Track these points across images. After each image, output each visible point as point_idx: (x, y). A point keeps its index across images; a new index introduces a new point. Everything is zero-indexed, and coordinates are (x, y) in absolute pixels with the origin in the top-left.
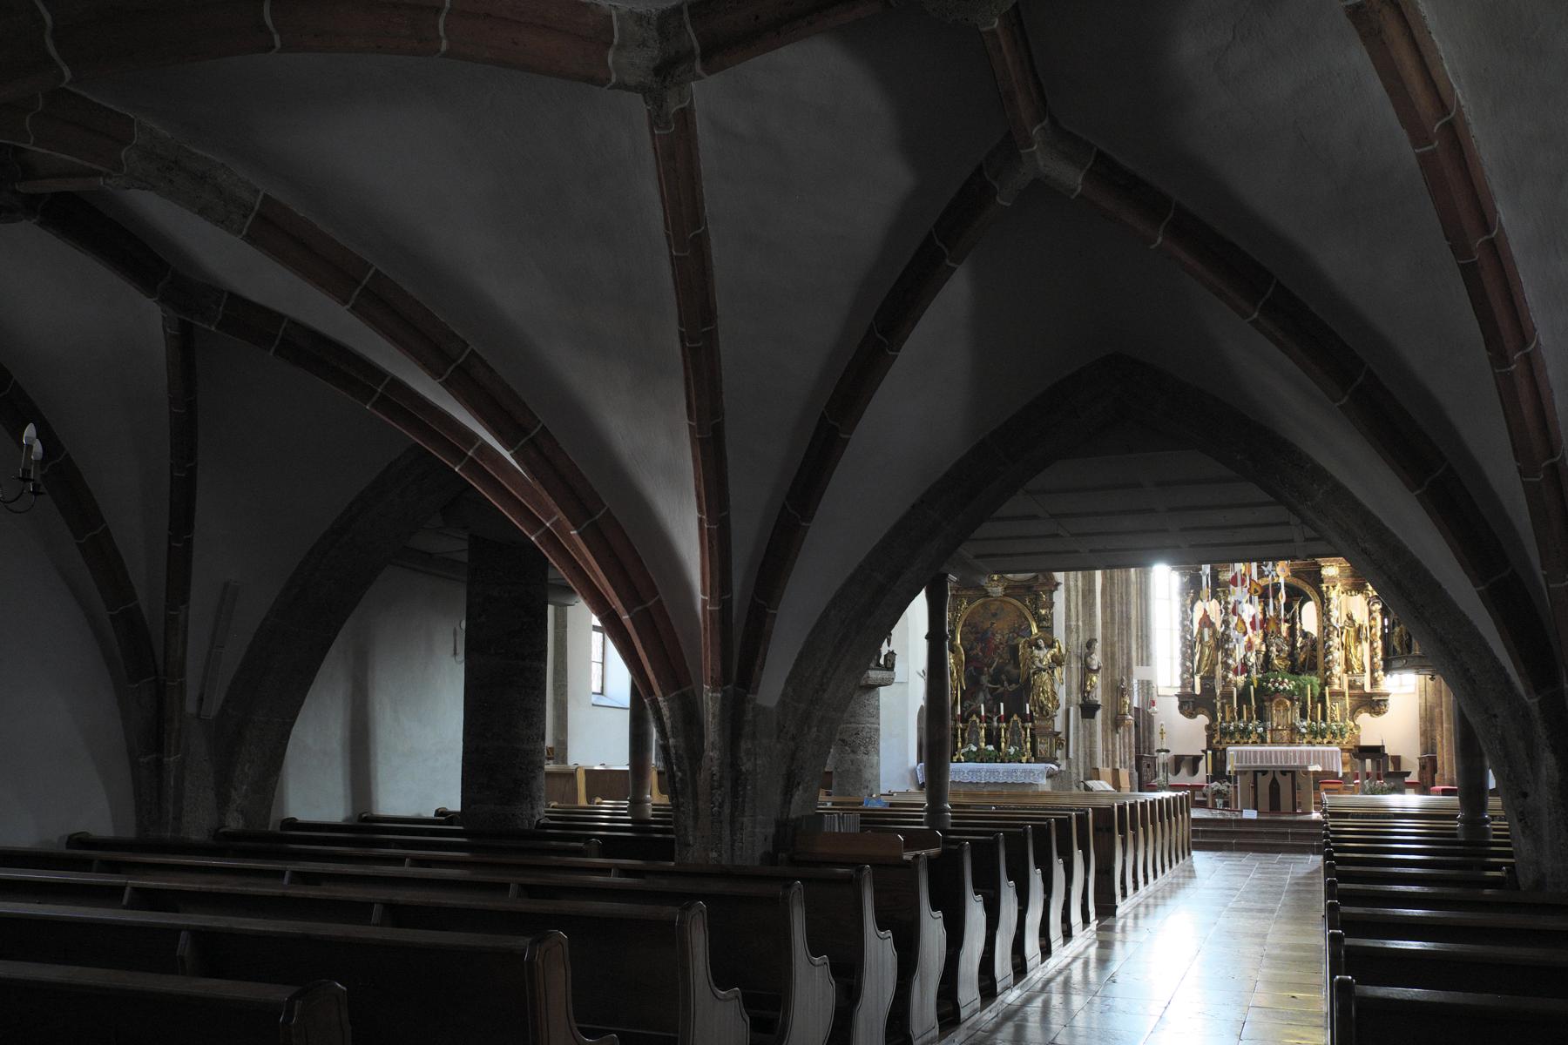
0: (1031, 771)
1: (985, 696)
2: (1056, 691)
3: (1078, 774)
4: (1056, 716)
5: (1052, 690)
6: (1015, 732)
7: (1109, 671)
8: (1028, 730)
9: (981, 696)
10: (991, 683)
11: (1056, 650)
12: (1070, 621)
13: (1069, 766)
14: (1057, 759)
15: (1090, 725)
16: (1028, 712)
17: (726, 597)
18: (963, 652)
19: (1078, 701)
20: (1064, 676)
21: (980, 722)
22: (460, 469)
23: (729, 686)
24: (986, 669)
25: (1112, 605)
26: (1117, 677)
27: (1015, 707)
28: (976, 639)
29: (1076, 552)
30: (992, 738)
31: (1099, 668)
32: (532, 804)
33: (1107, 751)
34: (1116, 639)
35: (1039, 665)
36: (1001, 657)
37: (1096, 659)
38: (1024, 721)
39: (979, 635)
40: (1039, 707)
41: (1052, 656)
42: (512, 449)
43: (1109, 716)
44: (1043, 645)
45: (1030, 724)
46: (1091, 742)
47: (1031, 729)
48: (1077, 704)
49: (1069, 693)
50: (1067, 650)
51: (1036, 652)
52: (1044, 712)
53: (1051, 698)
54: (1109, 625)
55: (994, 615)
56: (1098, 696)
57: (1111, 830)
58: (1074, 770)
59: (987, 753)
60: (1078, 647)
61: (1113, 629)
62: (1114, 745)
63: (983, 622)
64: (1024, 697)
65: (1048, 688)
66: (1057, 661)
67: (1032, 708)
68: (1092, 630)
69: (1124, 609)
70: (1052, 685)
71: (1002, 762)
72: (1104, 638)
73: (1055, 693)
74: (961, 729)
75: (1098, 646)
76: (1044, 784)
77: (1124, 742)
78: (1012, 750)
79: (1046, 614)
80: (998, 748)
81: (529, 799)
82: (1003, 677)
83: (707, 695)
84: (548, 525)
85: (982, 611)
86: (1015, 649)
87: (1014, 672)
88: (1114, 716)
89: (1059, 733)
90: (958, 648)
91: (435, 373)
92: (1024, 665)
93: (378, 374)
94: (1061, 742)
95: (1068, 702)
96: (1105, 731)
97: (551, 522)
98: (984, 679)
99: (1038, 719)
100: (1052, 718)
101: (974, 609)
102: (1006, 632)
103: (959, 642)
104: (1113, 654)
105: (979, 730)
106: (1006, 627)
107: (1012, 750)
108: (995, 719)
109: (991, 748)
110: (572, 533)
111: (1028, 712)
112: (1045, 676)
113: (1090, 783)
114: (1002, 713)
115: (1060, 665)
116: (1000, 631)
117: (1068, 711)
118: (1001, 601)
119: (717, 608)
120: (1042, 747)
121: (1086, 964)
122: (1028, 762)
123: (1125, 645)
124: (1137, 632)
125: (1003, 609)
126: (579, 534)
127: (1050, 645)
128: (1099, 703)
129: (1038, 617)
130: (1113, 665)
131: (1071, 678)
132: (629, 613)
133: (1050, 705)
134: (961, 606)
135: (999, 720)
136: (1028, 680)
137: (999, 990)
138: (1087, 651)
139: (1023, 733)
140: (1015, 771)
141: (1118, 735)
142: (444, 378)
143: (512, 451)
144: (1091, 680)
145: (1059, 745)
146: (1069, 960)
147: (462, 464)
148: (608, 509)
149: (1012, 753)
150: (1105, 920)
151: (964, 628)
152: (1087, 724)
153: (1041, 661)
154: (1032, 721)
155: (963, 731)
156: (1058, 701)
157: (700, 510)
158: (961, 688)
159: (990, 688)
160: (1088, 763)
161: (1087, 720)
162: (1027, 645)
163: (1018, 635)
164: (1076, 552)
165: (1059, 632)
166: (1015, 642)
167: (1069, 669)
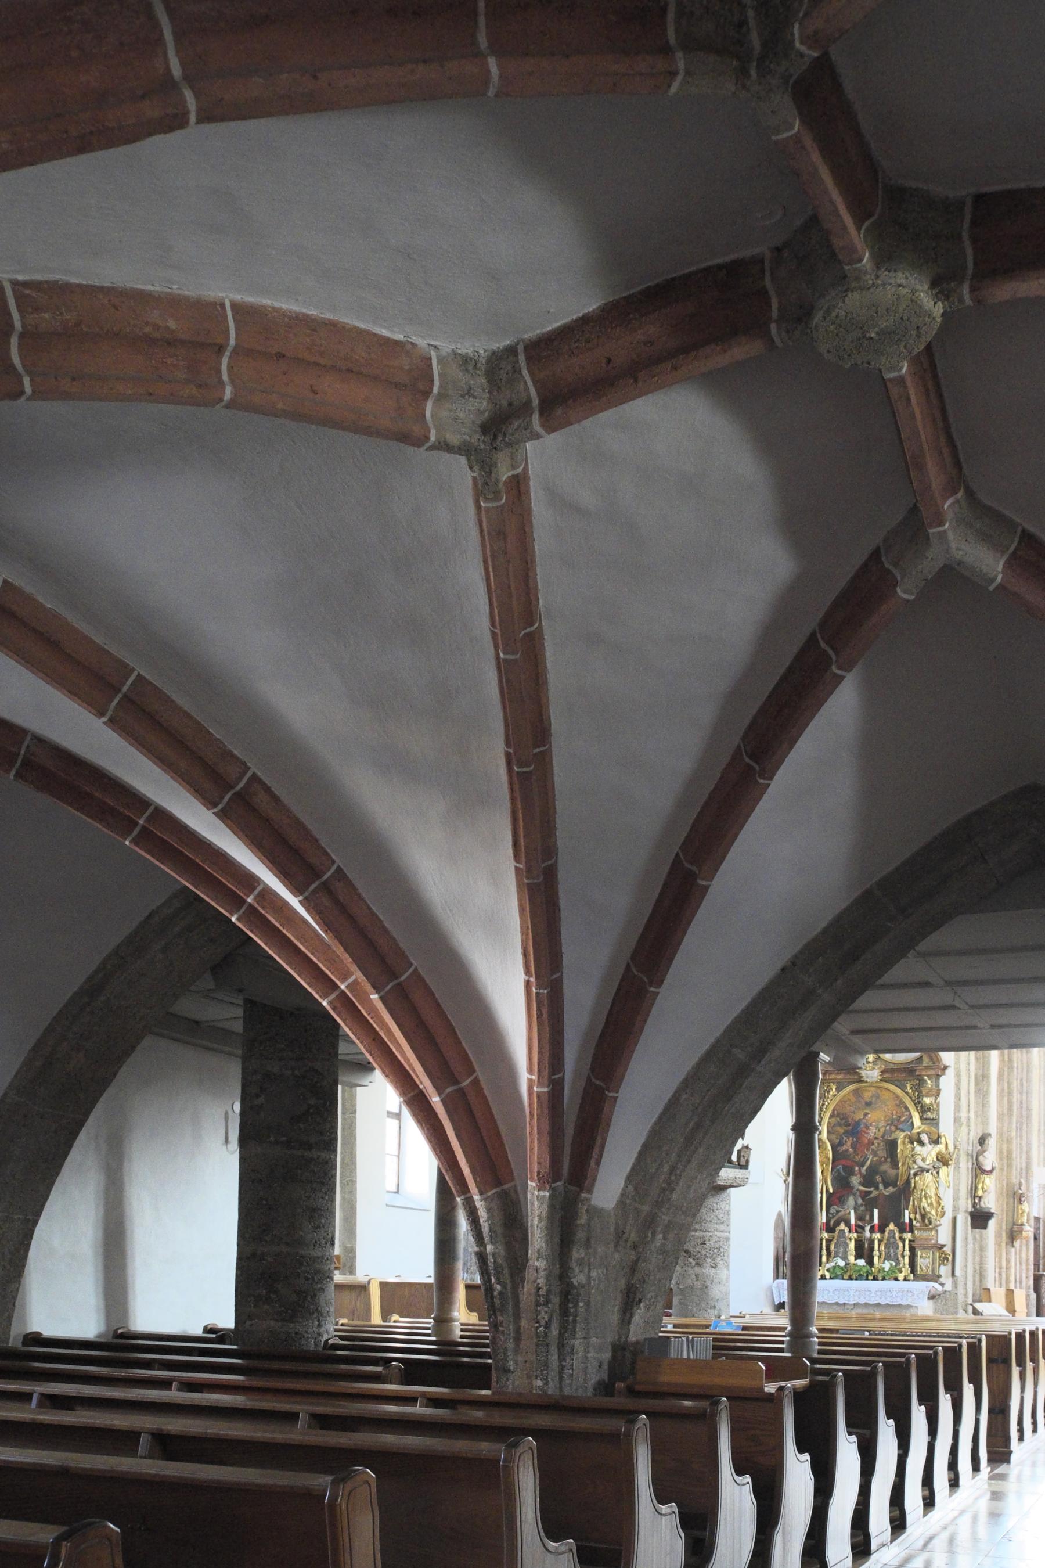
0: (909, 1291)
1: (856, 1202)
2: (941, 1196)
3: (966, 1295)
4: (940, 1225)
5: (936, 1195)
6: (891, 1244)
7: (1005, 1173)
8: (907, 1242)
9: (851, 1201)
10: (862, 1186)
11: (941, 1147)
13: (955, 1284)
14: (939, 1276)
15: (981, 1237)
16: (907, 1220)
17: (556, 1076)
19: (967, 1208)
20: (951, 1178)
21: (850, 1231)
22: (238, 919)
23: (559, 1183)
24: (857, 1168)
25: (1010, 1093)
26: (1015, 1180)
27: (892, 1212)
28: (846, 1132)
29: (975, 1027)
30: (863, 1250)
31: (993, 1169)
32: (318, 1321)
33: (1000, 1268)
34: (1014, 1134)
35: (922, 1164)
36: (875, 1153)
37: (989, 1160)
38: (902, 1231)
39: (850, 1128)
40: (921, 1213)
42: (301, 894)
43: (1004, 1227)
46: (981, 1257)
47: (910, 1241)
48: (966, 1211)
49: (956, 1199)
50: (955, 1147)
51: (918, 1149)
52: (926, 1221)
53: (935, 1204)
54: (1006, 1118)
55: (868, 1104)
56: (990, 1203)
57: (1007, 1362)
58: (961, 1291)
59: (857, 1268)
60: (968, 1144)
61: (1010, 1123)
62: (1008, 1261)
63: (854, 1112)
64: (903, 1202)
65: (931, 1192)
66: (943, 1160)
67: (912, 1216)
68: (985, 1122)
69: (1024, 1098)
70: (937, 1189)
71: (875, 1279)
72: (1000, 1134)
74: (827, 1240)
75: (992, 1143)
76: (926, 1308)
77: (1020, 1257)
78: (887, 1266)
80: (870, 1262)
81: (315, 1315)
82: (878, 1179)
83: (533, 1194)
84: (343, 987)
85: (853, 1099)
86: (892, 1145)
87: (892, 1172)
88: (1009, 1227)
89: (943, 1246)
91: (210, 803)
92: (903, 1164)
93: (141, 802)
94: (946, 1256)
95: (955, 1209)
96: (998, 1244)
97: (346, 983)
98: (855, 1181)
99: (918, 1229)
101: (844, 1096)
102: (882, 1124)
104: (1010, 1153)
105: (848, 1241)
106: (883, 1119)
107: (887, 1266)
108: (868, 1228)
109: (861, 1262)
110: (372, 997)
111: (907, 1220)
112: (928, 1177)
113: (979, 1306)
114: (876, 1221)
115: (946, 1163)
116: (876, 1122)
118: (878, 1087)
119: (546, 1090)
120: (923, 1262)
121: (975, 1519)
123: (1024, 1143)
124: (1039, 1126)
125: (878, 1097)
126: (381, 998)
127: (936, 1142)
128: (992, 1211)
129: (921, 1107)
130: (1009, 1165)
131: (959, 1179)
132: (440, 1095)
133: (933, 1212)
134: (828, 1092)
135: (872, 1230)
137: (873, 1547)
138: (979, 1148)
139: (901, 1245)
141: (1013, 1249)
142: (220, 807)
143: (301, 898)
145: (944, 1259)
146: (956, 1513)
147: (241, 911)
148: (416, 969)
149: (887, 1269)
150: (998, 1467)
151: (833, 1119)
152: (978, 1236)
153: (923, 1160)
154: (912, 1231)
155: (829, 1241)
156: (942, 1209)
157: (527, 971)
158: (827, 1191)
159: (861, 1191)
160: (978, 1283)
161: (977, 1230)
162: (907, 1140)
163: (897, 1129)
164: (975, 1027)
165: (946, 1127)
166: (893, 1136)
167: (957, 1168)
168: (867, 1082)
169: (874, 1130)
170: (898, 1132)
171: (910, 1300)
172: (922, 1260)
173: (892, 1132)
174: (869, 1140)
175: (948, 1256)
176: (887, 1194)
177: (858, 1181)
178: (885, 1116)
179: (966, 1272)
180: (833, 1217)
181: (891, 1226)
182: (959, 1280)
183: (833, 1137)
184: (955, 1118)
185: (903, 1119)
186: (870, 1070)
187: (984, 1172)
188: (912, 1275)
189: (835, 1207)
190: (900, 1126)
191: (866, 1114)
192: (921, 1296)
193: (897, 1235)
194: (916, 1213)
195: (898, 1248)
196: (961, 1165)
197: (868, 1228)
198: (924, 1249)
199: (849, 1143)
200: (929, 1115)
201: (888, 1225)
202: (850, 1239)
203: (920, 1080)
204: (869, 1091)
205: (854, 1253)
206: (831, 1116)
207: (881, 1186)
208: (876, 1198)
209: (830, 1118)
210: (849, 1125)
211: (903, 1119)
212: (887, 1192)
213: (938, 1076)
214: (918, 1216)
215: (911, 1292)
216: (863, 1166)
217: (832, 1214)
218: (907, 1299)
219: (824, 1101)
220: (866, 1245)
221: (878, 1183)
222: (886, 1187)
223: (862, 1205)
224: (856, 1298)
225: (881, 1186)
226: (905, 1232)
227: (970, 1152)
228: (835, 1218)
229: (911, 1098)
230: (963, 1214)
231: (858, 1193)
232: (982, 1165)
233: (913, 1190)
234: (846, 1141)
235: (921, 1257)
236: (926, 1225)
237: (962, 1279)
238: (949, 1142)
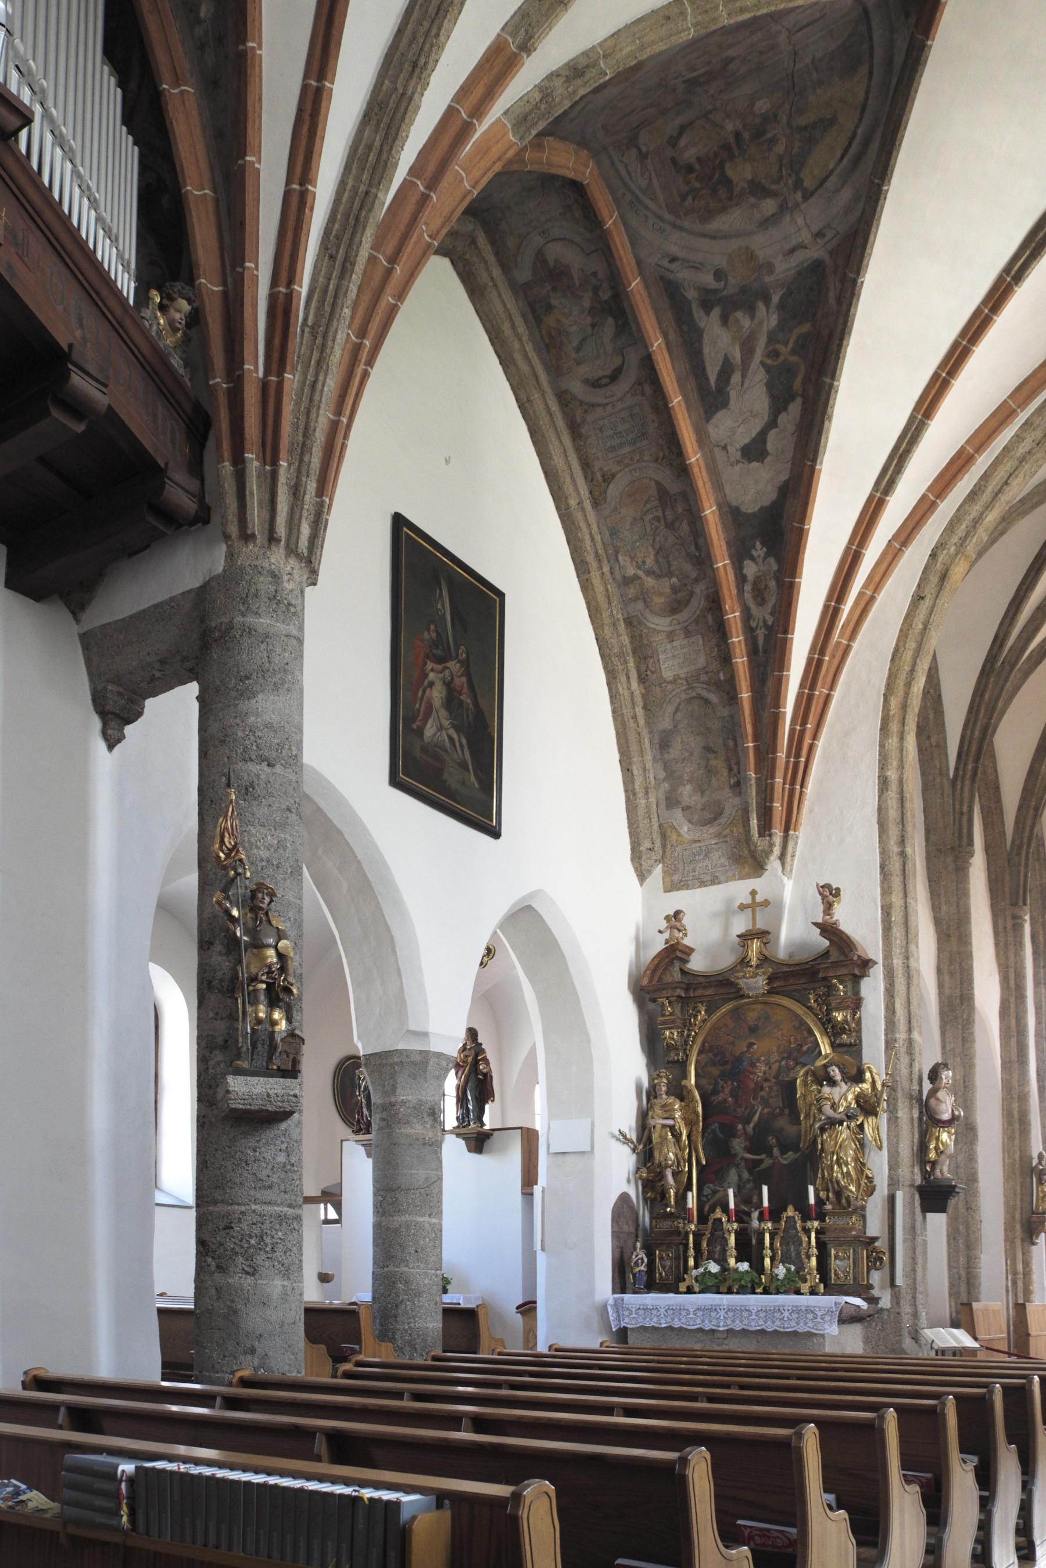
0: (809, 1310)
6: (790, 1239)
8: (813, 1235)
9: (733, 1175)
10: (749, 1152)
11: (866, 1086)
12: (893, 1032)
13: (896, 1299)
18: (698, 1097)
19: (913, 1180)
21: (728, 1221)
28: (723, 1075)
30: (748, 1249)
36: (765, 1103)
38: (806, 1217)
39: (728, 1067)
41: (858, 1098)
44: (838, 1077)
45: (816, 1224)
47: (818, 1232)
48: (912, 1186)
49: (893, 1165)
51: (826, 1090)
52: (844, 1201)
55: (753, 1030)
60: (911, 1080)
64: (810, 1173)
66: (867, 1107)
73: (863, 1164)
78: (781, 1271)
79: (845, 1021)
80: (758, 1267)
82: (772, 1140)
87: (791, 1130)
89: (874, 1239)
90: (690, 1092)
92: (807, 1116)
95: (894, 1183)
98: (738, 1145)
99: (833, 1214)
101: (719, 1020)
102: (775, 1057)
103: (693, 1081)
106: (775, 1049)
107: (781, 1271)
108: (755, 1214)
109: (744, 1266)
112: (844, 1133)
114: (766, 1203)
117: (891, 1200)
118: (766, 1003)
122: (813, 1292)
127: (858, 1077)
129: (833, 1027)
131: (897, 1136)
134: (695, 1017)
135: (761, 1219)
136: (815, 1142)
140: (779, 1309)
144: (938, 1139)
145: (875, 1261)
149: (781, 1277)
151: (703, 1056)
154: (821, 1217)
155: (698, 1236)
159: (747, 1160)
163: (797, 1063)
168: (749, 997)
169: (763, 1068)
170: (798, 1068)
171: (810, 1324)
172: (837, 1262)
173: (790, 1069)
174: (756, 1084)
175: (881, 1255)
176: (785, 1162)
177: (743, 1145)
178: (779, 1046)
179: (915, 1279)
180: (709, 1200)
182: (903, 1291)
183: (704, 1082)
184: (887, 1042)
185: (805, 1048)
186: (751, 977)
188: (822, 1286)
189: (711, 1185)
190: (802, 1060)
191: (751, 1045)
192: (827, 1318)
193: (799, 1224)
194: (828, 1190)
195: (801, 1244)
196: (900, 1114)
197: (755, 1214)
198: (841, 1245)
199: (727, 1091)
201: (786, 1210)
202: (729, 1232)
203: (828, 987)
204: (754, 1010)
205: (734, 1252)
206: (700, 1052)
207: (776, 1151)
208: (769, 1169)
209: (698, 1055)
210: (727, 1062)
211: (805, 1048)
212: (786, 1159)
213: (857, 979)
214: (831, 1195)
215: (812, 1312)
216: (747, 1121)
217: (707, 1196)
218: (806, 1324)
219: (689, 1030)
220: (754, 1241)
221: (772, 1148)
222: (784, 1151)
223: (749, 1181)
224: (729, 1322)
225: (776, 1151)
226: (811, 1219)
227: (915, 1093)
228: (711, 1202)
229: (816, 1015)
230: (907, 1189)
231: (743, 1164)
232: (936, 1113)
233: (821, 1155)
234: (722, 1087)
235: (837, 1257)
236: (844, 1208)
237: (909, 1291)
238: (876, 1077)
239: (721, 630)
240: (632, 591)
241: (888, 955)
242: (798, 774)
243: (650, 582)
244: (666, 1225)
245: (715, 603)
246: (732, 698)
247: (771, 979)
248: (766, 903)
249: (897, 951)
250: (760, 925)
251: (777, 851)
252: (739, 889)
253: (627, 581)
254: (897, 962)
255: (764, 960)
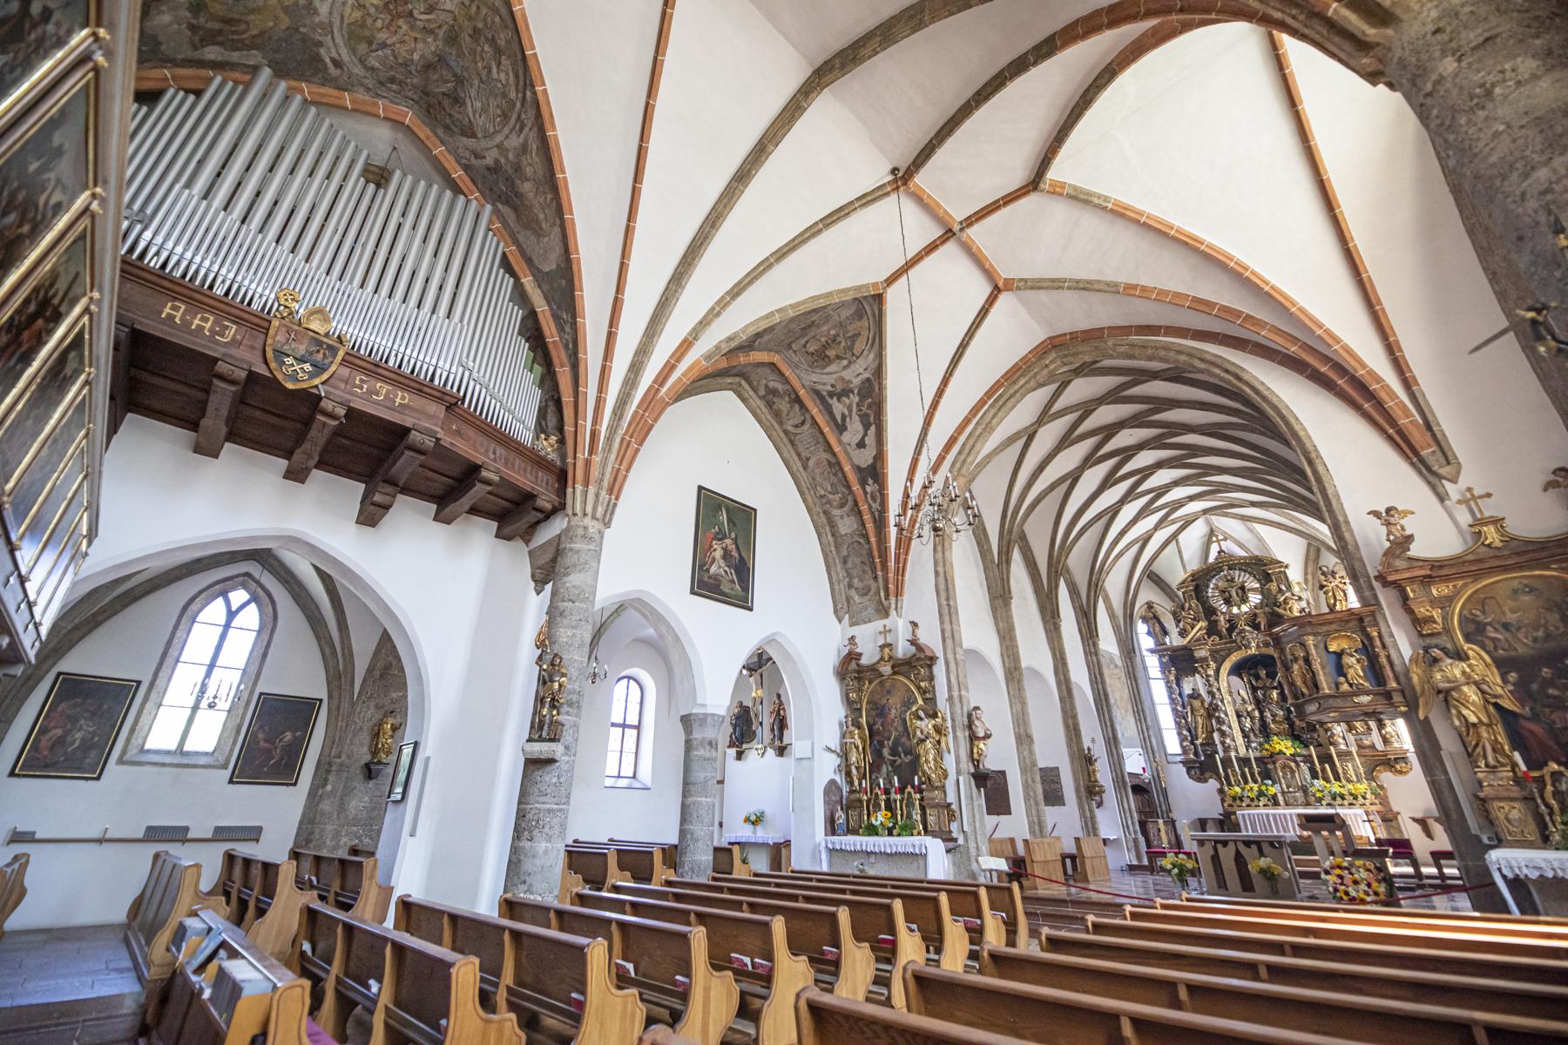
36: (896, 729)
82: (900, 749)
87: (908, 743)
98: (886, 752)
100: (943, 789)
181: (909, 789)
187: (979, 739)
200: (928, 696)
213: (930, 667)
239: (860, 513)
240: (824, 501)
241: (945, 654)
242: (901, 571)
243: (830, 496)
244: (854, 796)
245: (856, 503)
246: (868, 542)
247: (893, 667)
248: (890, 631)
249: (949, 651)
250: (889, 641)
251: (893, 606)
252: (879, 624)
253: (822, 497)
254: (950, 656)
255: (891, 658)
